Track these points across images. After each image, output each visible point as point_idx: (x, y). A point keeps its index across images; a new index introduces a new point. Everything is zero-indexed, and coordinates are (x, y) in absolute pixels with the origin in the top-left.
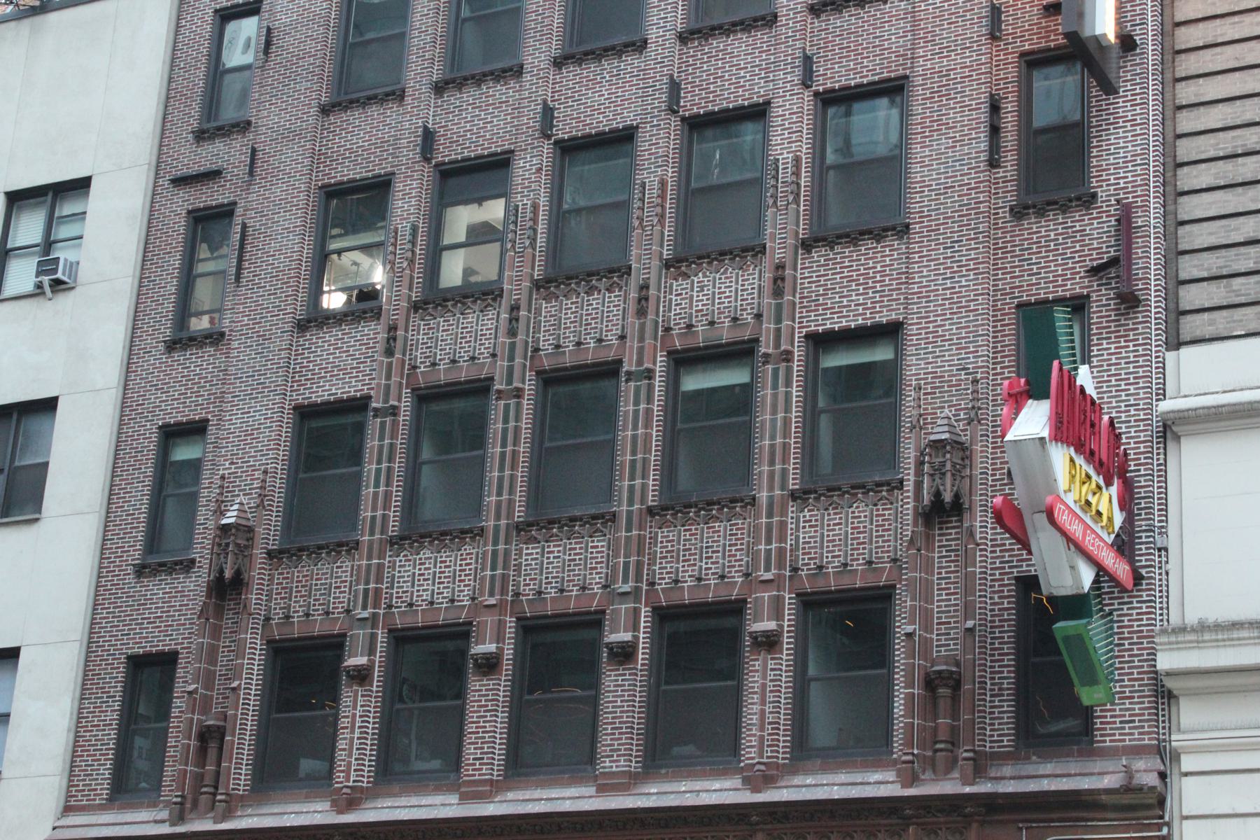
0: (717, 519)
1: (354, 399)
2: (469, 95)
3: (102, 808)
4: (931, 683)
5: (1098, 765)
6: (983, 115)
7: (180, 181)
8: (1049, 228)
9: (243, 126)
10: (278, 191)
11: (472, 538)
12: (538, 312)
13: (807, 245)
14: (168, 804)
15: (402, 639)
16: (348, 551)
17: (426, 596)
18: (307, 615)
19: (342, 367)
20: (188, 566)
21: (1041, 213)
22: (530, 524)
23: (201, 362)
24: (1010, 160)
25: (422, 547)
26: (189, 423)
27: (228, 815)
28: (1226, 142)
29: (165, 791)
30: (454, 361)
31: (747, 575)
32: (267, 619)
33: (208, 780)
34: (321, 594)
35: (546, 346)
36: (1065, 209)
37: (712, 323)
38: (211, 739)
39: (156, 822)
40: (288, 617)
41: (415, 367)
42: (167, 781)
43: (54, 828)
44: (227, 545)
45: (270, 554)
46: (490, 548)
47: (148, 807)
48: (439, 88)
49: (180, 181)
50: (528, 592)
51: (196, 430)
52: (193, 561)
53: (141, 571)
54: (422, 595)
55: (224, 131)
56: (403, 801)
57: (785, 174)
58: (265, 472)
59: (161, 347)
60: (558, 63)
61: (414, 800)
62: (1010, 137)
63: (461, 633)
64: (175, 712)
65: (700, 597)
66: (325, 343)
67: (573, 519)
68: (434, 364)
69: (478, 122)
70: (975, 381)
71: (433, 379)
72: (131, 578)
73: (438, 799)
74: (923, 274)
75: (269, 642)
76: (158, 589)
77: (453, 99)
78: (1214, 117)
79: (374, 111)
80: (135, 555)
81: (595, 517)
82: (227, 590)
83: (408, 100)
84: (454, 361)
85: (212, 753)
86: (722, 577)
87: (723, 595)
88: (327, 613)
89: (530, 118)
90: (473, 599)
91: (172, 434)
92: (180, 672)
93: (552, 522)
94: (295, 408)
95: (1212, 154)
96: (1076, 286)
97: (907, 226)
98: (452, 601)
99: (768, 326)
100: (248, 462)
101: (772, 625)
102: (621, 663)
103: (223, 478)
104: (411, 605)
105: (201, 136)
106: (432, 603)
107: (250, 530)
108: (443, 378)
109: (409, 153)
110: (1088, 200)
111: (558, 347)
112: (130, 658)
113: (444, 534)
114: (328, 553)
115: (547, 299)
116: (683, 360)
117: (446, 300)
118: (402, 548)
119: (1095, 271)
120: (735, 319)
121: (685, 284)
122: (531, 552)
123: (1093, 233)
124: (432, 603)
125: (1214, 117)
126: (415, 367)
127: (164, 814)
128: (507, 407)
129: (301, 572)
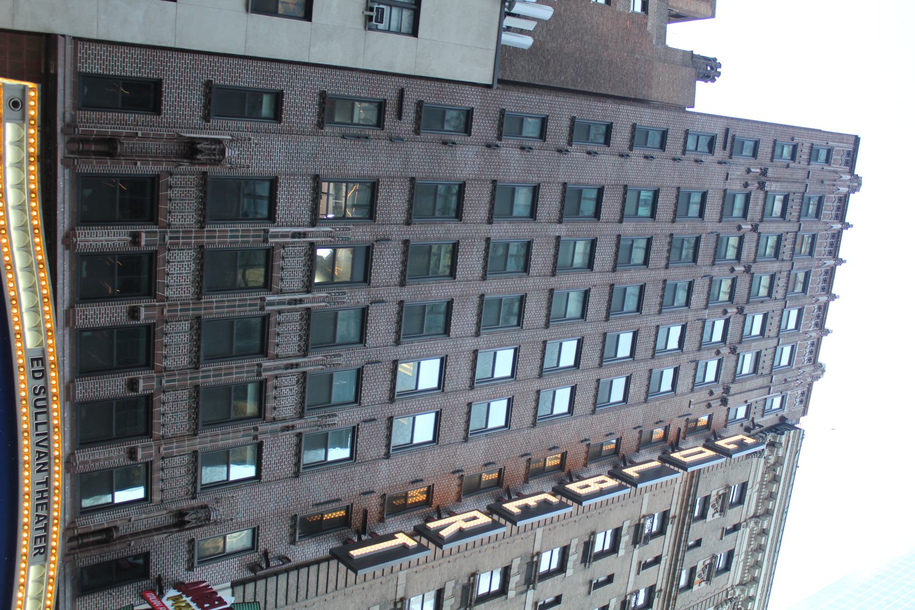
0: (190, 417)
1: (275, 214)
2: (399, 258)
3: (75, 67)
4: (108, 531)
5: (68, 603)
6: (335, 497)
7: (402, 92)
8: (286, 530)
9: (417, 131)
10: (383, 158)
11: (197, 293)
12: (296, 310)
13: (299, 435)
14: (74, 117)
15: (152, 257)
16: (200, 222)
17: (172, 271)
18: (170, 200)
19: (292, 201)
20: (206, 118)
21: (291, 527)
22: (200, 324)
23: (310, 116)
24: (316, 510)
25: (198, 264)
26: (282, 110)
27: (66, 166)
28: (303, 585)
29: (81, 113)
30: (283, 269)
31: (163, 436)
32: (171, 174)
33: (86, 147)
34: (181, 207)
35: (280, 318)
36: (293, 535)
37: (275, 398)
38: (109, 146)
39: (64, 113)
40: (171, 187)
41: (284, 247)
42: (88, 114)
43: (64, 36)
44: (214, 155)
45: (205, 173)
46: (191, 306)
47: (74, 104)
48: (406, 242)
49: (402, 92)
50: (167, 328)
51: (277, 115)
52: (209, 121)
53: (208, 85)
54: (173, 269)
55: (418, 119)
56: (67, 274)
57: (329, 421)
58: (248, 167)
59: (324, 89)
60: (401, 303)
61: (67, 282)
62: (322, 508)
63: (150, 291)
64: (127, 116)
65: (155, 415)
66: (304, 193)
67: (199, 347)
68: (283, 258)
69: (387, 264)
70: (232, 519)
71: (276, 258)
72: (205, 78)
73: (67, 296)
74: (277, 488)
75: (159, 175)
76: (196, 99)
77: (399, 248)
78: (313, 578)
79: (406, 206)
80: (218, 81)
81: (198, 358)
82: (190, 150)
83: (405, 228)
84: (283, 269)
85: (101, 148)
86: (163, 425)
87: (155, 427)
88: (170, 212)
89: (382, 293)
90: (167, 298)
91: (278, 97)
92: (149, 118)
93: (199, 336)
94: (277, 177)
95: (300, 580)
96: (262, 546)
97: (297, 476)
98: (168, 286)
99: (270, 427)
100: (253, 151)
101: (139, 456)
102: (128, 386)
103: (250, 139)
104: (168, 262)
105: (420, 104)
106: (168, 274)
107: (220, 161)
108: (276, 264)
109: (382, 231)
110: (293, 542)
111: (279, 324)
112: (161, 80)
113: (201, 277)
114: (200, 209)
115: (301, 315)
116: (262, 387)
117: (312, 261)
118: (198, 252)
119: (266, 554)
120: (275, 408)
121: (294, 382)
122: (186, 326)
123: (281, 549)
124: (168, 274)
125: (313, 578)
126: (284, 247)
127: (68, 116)
128: (256, 305)
129: (194, 192)
